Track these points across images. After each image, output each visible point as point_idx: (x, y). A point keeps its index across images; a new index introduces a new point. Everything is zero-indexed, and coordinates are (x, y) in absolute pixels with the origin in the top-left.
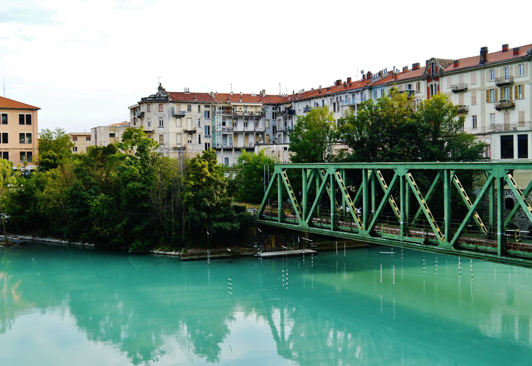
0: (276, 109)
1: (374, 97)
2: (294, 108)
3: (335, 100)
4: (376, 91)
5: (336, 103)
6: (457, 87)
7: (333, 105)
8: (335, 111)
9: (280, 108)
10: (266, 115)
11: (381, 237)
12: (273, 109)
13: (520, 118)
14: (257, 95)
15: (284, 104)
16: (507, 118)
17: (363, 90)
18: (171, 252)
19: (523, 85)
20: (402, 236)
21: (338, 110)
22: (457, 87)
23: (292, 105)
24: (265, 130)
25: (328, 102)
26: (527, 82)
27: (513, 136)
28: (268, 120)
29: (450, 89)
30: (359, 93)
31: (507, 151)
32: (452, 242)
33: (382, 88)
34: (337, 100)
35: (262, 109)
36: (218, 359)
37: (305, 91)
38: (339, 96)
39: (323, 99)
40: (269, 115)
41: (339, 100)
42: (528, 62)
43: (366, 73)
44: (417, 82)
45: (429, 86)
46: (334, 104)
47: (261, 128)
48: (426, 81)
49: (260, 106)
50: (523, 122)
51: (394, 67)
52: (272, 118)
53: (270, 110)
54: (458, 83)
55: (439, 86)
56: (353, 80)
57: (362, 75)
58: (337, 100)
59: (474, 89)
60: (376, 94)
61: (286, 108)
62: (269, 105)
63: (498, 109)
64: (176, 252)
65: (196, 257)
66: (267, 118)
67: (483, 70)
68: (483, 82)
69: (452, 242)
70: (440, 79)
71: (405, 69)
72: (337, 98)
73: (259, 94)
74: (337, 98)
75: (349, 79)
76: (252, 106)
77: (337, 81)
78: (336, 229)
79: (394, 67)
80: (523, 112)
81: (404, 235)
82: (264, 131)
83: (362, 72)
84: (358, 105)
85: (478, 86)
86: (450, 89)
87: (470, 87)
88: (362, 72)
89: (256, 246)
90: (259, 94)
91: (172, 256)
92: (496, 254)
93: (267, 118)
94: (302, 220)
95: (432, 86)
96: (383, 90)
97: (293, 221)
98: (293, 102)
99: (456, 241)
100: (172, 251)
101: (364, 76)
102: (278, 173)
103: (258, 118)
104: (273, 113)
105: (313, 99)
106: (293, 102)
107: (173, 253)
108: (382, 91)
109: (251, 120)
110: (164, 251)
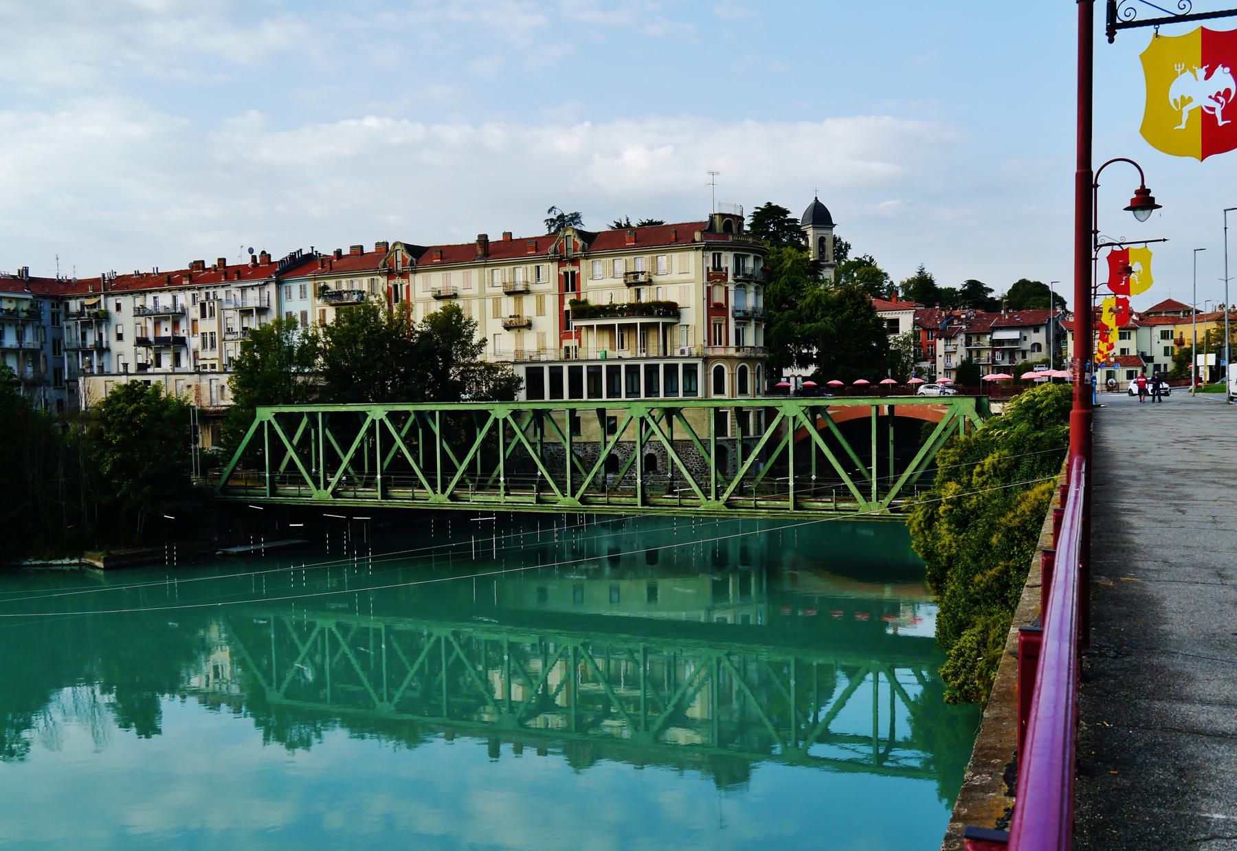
0: (58, 307)
1: (287, 298)
2: (106, 306)
3: (203, 298)
4: (290, 287)
5: (207, 303)
6: (439, 291)
7: (198, 305)
8: (203, 316)
9: (67, 305)
10: (43, 318)
11: (469, 501)
12: (53, 306)
13: (538, 343)
14: (12, 276)
15: (77, 298)
16: (519, 342)
17: (265, 284)
18: (61, 559)
19: (544, 295)
20: (502, 495)
21: (212, 314)
22: (439, 291)
23: (100, 301)
24: (42, 346)
25: (186, 299)
26: (548, 292)
27: (543, 368)
28: (44, 327)
29: (430, 293)
30: (257, 290)
31: (535, 391)
32: (578, 496)
33: (302, 283)
34: (207, 298)
35: (31, 305)
36: (159, 732)
37: (117, 275)
38: (211, 291)
39: (175, 293)
40: (46, 317)
41: (211, 297)
42: (550, 264)
43: (257, 253)
44: (370, 278)
45: (391, 286)
46: (203, 306)
47: (29, 340)
48: (386, 278)
49: (27, 299)
50: (544, 349)
51: (312, 248)
52: (50, 323)
53: (46, 307)
54: (441, 285)
55: (408, 288)
56: (228, 264)
57: (250, 256)
58: (207, 298)
59: (467, 296)
60: (290, 292)
61: (82, 305)
62: (44, 297)
63: (508, 328)
64: (72, 558)
65: (126, 562)
66: (43, 323)
67: (483, 269)
68: (482, 286)
69: (578, 496)
70: (411, 276)
71: (338, 253)
72: (207, 294)
73: (16, 274)
74: (207, 294)
75: (222, 261)
76: (10, 300)
77: (195, 262)
78: (385, 495)
79: (312, 248)
80: (544, 334)
81: (505, 495)
82: (39, 347)
83: (251, 251)
84: (256, 308)
85: (475, 291)
86: (430, 293)
87: (461, 292)
88: (251, 251)
89: (216, 538)
90: (16, 274)
91: (64, 567)
92: (636, 505)
93: (43, 323)
94: (318, 488)
95: (396, 286)
96: (304, 285)
97: (297, 492)
98: (102, 296)
99: (582, 496)
100: (64, 558)
101: (254, 258)
102: (265, 420)
103: (25, 323)
104: (53, 314)
105: (151, 292)
106: (102, 296)
107: (66, 561)
108: (301, 288)
109: (10, 325)
110: (43, 560)
